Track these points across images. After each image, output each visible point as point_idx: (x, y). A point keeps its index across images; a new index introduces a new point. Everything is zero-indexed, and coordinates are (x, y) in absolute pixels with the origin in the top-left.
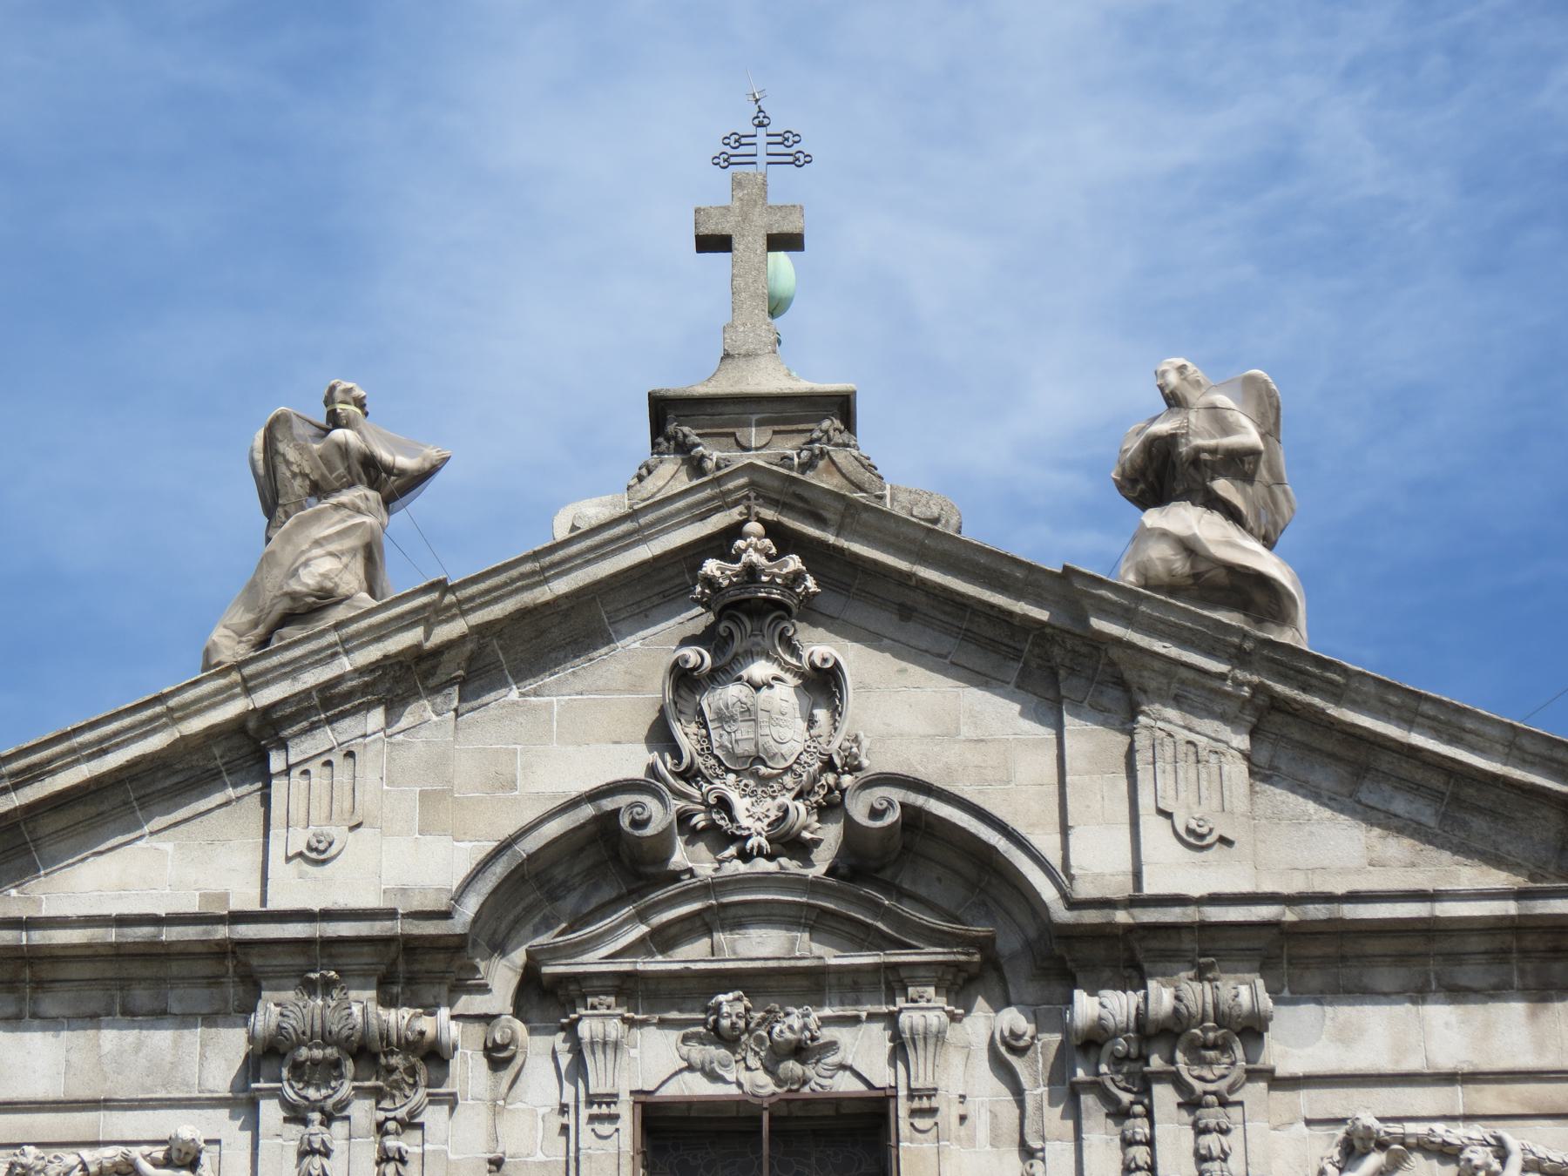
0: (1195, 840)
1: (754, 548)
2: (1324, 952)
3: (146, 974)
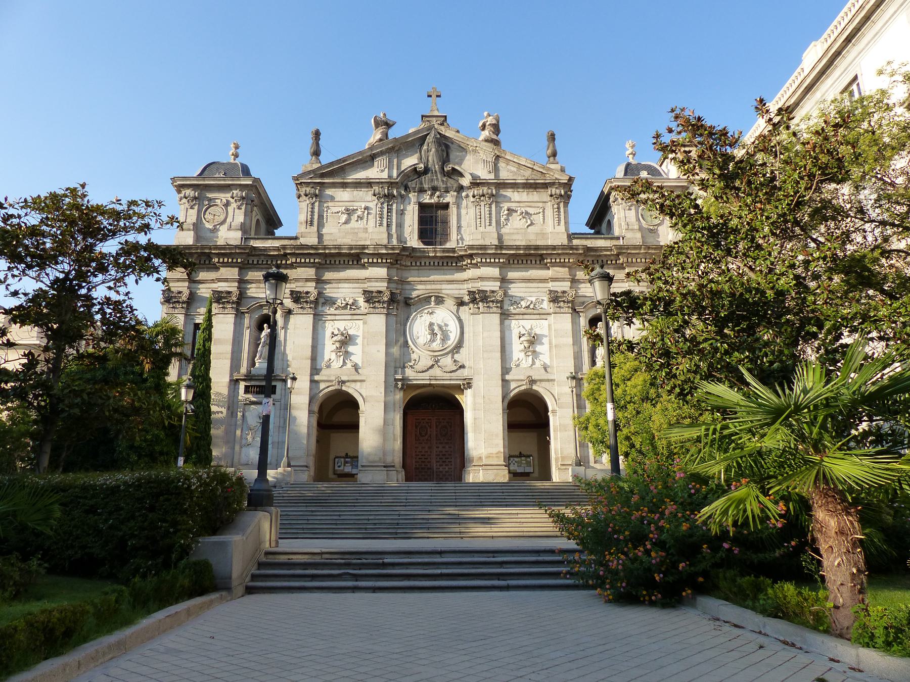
3: (358, 185)
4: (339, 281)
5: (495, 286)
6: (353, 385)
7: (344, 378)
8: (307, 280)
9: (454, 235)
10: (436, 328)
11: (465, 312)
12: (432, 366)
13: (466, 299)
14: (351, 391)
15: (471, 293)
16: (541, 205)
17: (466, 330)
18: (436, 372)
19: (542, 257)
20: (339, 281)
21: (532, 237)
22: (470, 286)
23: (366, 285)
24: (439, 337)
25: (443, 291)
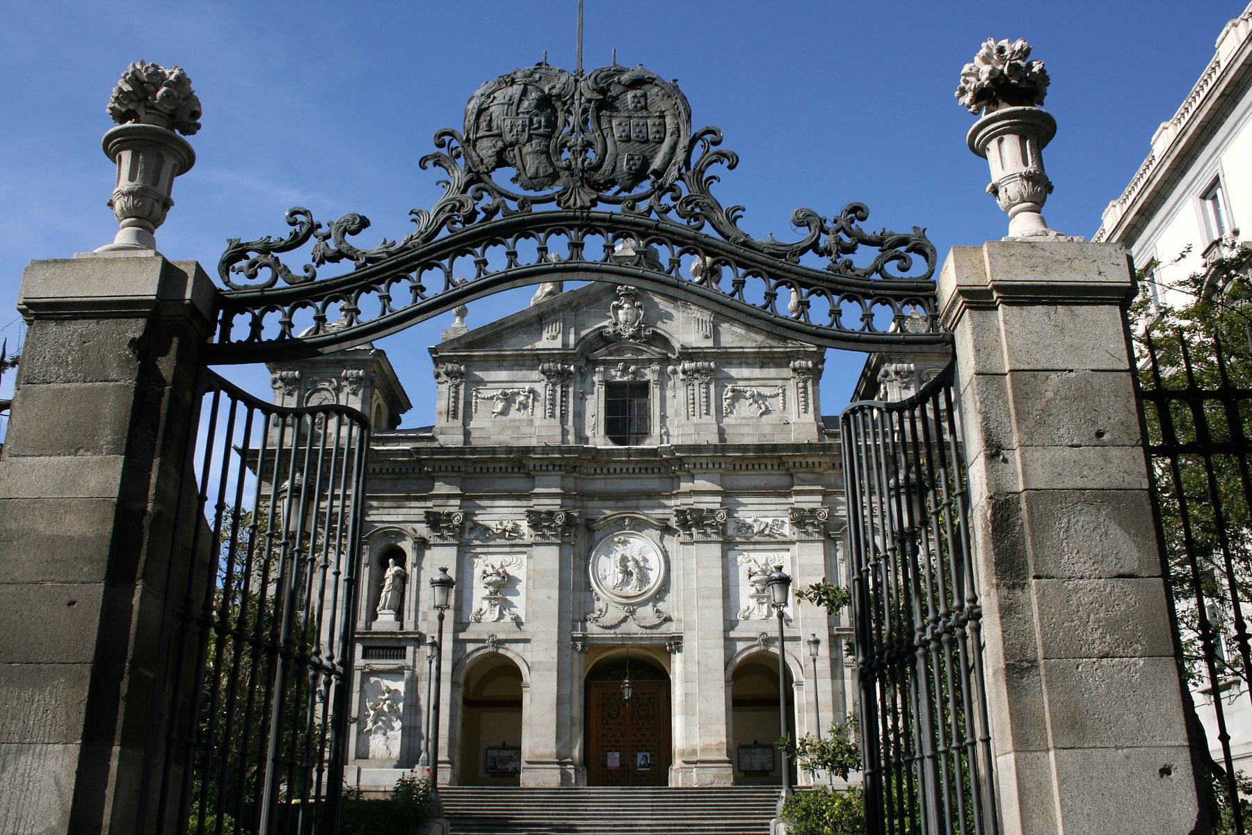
5: (713, 502)
6: (513, 646)
7: (501, 636)
9: (656, 430)
10: (631, 565)
11: (671, 543)
12: (625, 620)
13: (673, 522)
14: (510, 655)
15: (680, 513)
16: (780, 383)
17: (673, 565)
18: (631, 627)
21: (767, 430)
22: (678, 502)
23: (531, 503)
24: (634, 577)
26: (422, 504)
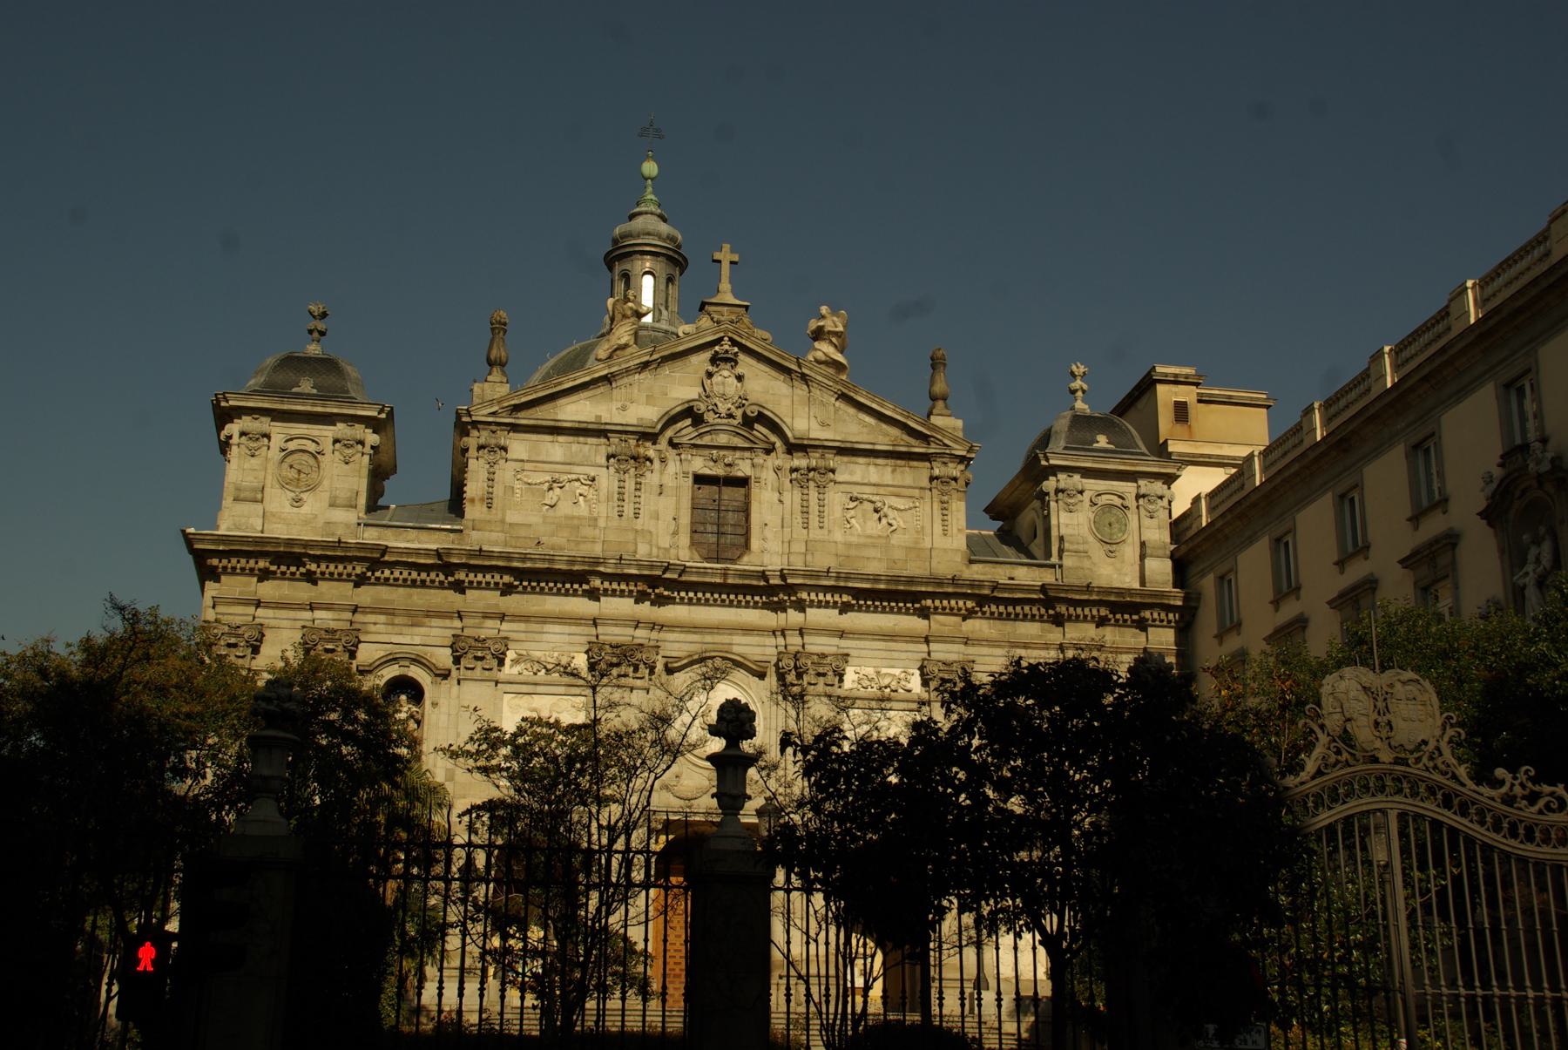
0: (823, 425)
1: (726, 345)
2: (848, 451)
4: (545, 619)
8: (486, 616)
9: (755, 543)
16: (916, 493)
19: (916, 597)
20: (545, 619)
21: (898, 554)
25: (736, 649)
26: (447, 623)
